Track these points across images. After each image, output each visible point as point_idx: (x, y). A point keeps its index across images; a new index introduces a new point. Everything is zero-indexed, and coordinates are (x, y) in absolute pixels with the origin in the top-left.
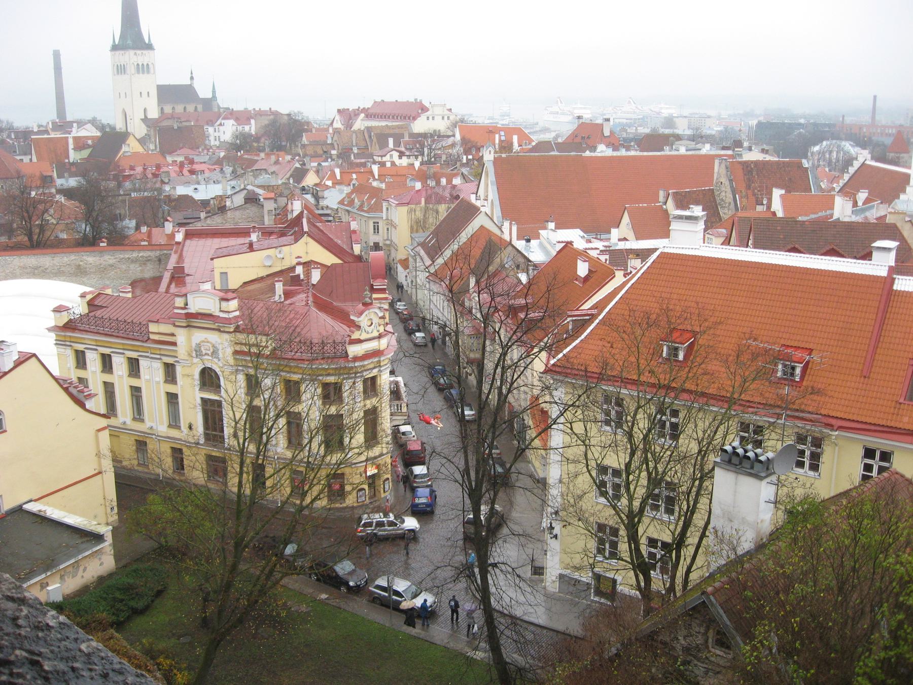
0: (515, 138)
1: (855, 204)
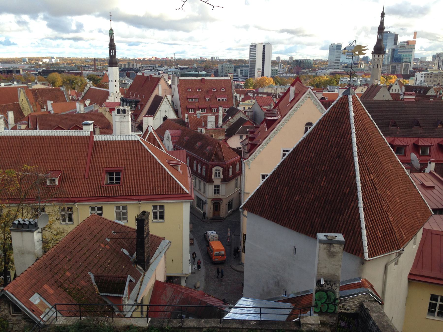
1: (85, 106)
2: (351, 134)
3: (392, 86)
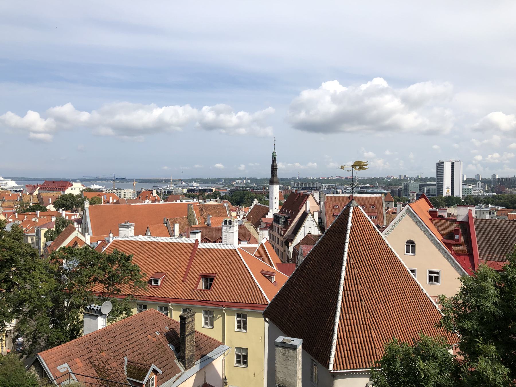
0: (111, 197)
2: (345, 244)
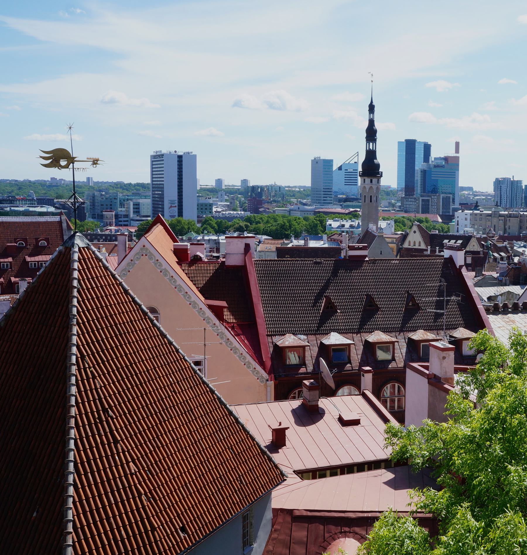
3: (408, 234)
